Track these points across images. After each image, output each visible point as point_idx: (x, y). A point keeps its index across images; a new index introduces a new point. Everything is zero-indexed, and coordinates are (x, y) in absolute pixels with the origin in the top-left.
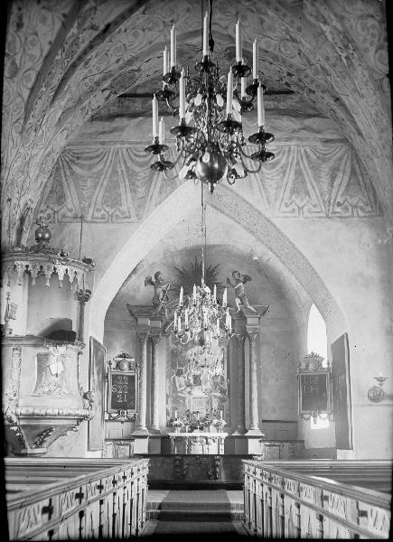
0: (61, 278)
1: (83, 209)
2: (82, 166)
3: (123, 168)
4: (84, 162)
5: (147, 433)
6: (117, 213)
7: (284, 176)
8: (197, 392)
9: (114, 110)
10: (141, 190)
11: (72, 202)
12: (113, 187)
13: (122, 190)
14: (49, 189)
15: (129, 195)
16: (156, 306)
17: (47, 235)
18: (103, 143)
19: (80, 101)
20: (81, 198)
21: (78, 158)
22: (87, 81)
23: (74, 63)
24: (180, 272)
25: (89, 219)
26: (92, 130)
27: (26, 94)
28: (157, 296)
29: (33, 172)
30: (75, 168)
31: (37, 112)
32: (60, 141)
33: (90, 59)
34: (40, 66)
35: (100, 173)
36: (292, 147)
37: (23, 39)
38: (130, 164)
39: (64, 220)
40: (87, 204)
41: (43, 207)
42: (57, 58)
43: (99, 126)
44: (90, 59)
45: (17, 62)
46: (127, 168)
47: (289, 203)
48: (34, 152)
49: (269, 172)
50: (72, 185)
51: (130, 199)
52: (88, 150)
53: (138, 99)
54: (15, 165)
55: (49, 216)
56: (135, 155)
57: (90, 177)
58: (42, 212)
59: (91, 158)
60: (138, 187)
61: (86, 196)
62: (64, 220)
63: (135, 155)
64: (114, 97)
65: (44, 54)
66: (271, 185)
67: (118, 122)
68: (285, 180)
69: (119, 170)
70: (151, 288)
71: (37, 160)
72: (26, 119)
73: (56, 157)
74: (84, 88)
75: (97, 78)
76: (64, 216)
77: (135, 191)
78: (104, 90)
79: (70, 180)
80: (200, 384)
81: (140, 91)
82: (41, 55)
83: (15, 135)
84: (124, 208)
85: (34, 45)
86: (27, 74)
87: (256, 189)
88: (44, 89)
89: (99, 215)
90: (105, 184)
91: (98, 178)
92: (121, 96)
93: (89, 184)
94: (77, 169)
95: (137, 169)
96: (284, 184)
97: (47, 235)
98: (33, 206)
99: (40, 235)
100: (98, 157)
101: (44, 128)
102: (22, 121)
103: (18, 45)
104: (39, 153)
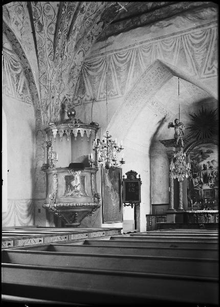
0: (82, 135)
1: (94, 95)
2: (92, 70)
3: (114, 67)
4: (93, 68)
5: (175, 211)
6: (112, 93)
7: (207, 50)
8: (206, 187)
9: (108, 32)
10: (123, 77)
11: (89, 92)
12: (109, 78)
13: (113, 79)
14: (78, 87)
15: (117, 81)
16: (176, 139)
17: (73, 113)
18: (102, 54)
19: (85, 33)
20: (93, 89)
21: (91, 66)
22: (87, 20)
23: (76, 12)
24: (193, 117)
25: (98, 99)
26: (98, 47)
27: (52, 38)
28: (176, 134)
29: (65, 80)
30: (90, 72)
31: (59, 47)
32: (79, 59)
33: (84, 7)
34: (56, 20)
35: (102, 72)
36: (213, 29)
37: (40, 9)
38: (116, 62)
39: (86, 102)
40: (96, 92)
41: (76, 97)
42: (63, 13)
43: (101, 44)
44: (84, 7)
45: (41, 22)
46: (115, 65)
47: (211, 67)
48: (64, 68)
49: (198, 49)
50: (89, 83)
51: (117, 83)
52: (95, 60)
53: (120, 22)
54: (54, 78)
55: (79, 101)
56: (119, 57)
57: (97, 76)
58: (76, 99)
59: (97, 64)
60: (121, 76)
61: (95, 87)
62: (86, 102)
63: (119, 57)
64: (107, 25)
65: (57, 13)
66: (199, 58)
67: (111, 39)
68: (208, 52)
69: (111, 68)
70: (172, 129)
71: (67, 72)
72: (55, 51)
73: (80, 68)
74: (87, 24)
75: (92, 17)
76: (86, 100)
77: (119, 79)
78: (98, 23)
79: (88, 80)
80: (208, 182)
81: (122, 17)
82: (55, 14)
83: (50, 62)
84: (115, 90)
85: (49, 10)
86: (50, 27)
87: (189, 63)
88: (60, 33)
89: (102, 96)
90: (104, 78)
91: (101, 75)
92: (112, 23)
93: (97, 80)
94: (90, 72)
95: (121, 65)
96: (207, 56)
97: (73, 113)
98: (71, 97)
99: (69, 114)
100: (99, 63)
101: (66, 54)
102: (53, 54)
103: (38, 11)
104: (67, 68)
